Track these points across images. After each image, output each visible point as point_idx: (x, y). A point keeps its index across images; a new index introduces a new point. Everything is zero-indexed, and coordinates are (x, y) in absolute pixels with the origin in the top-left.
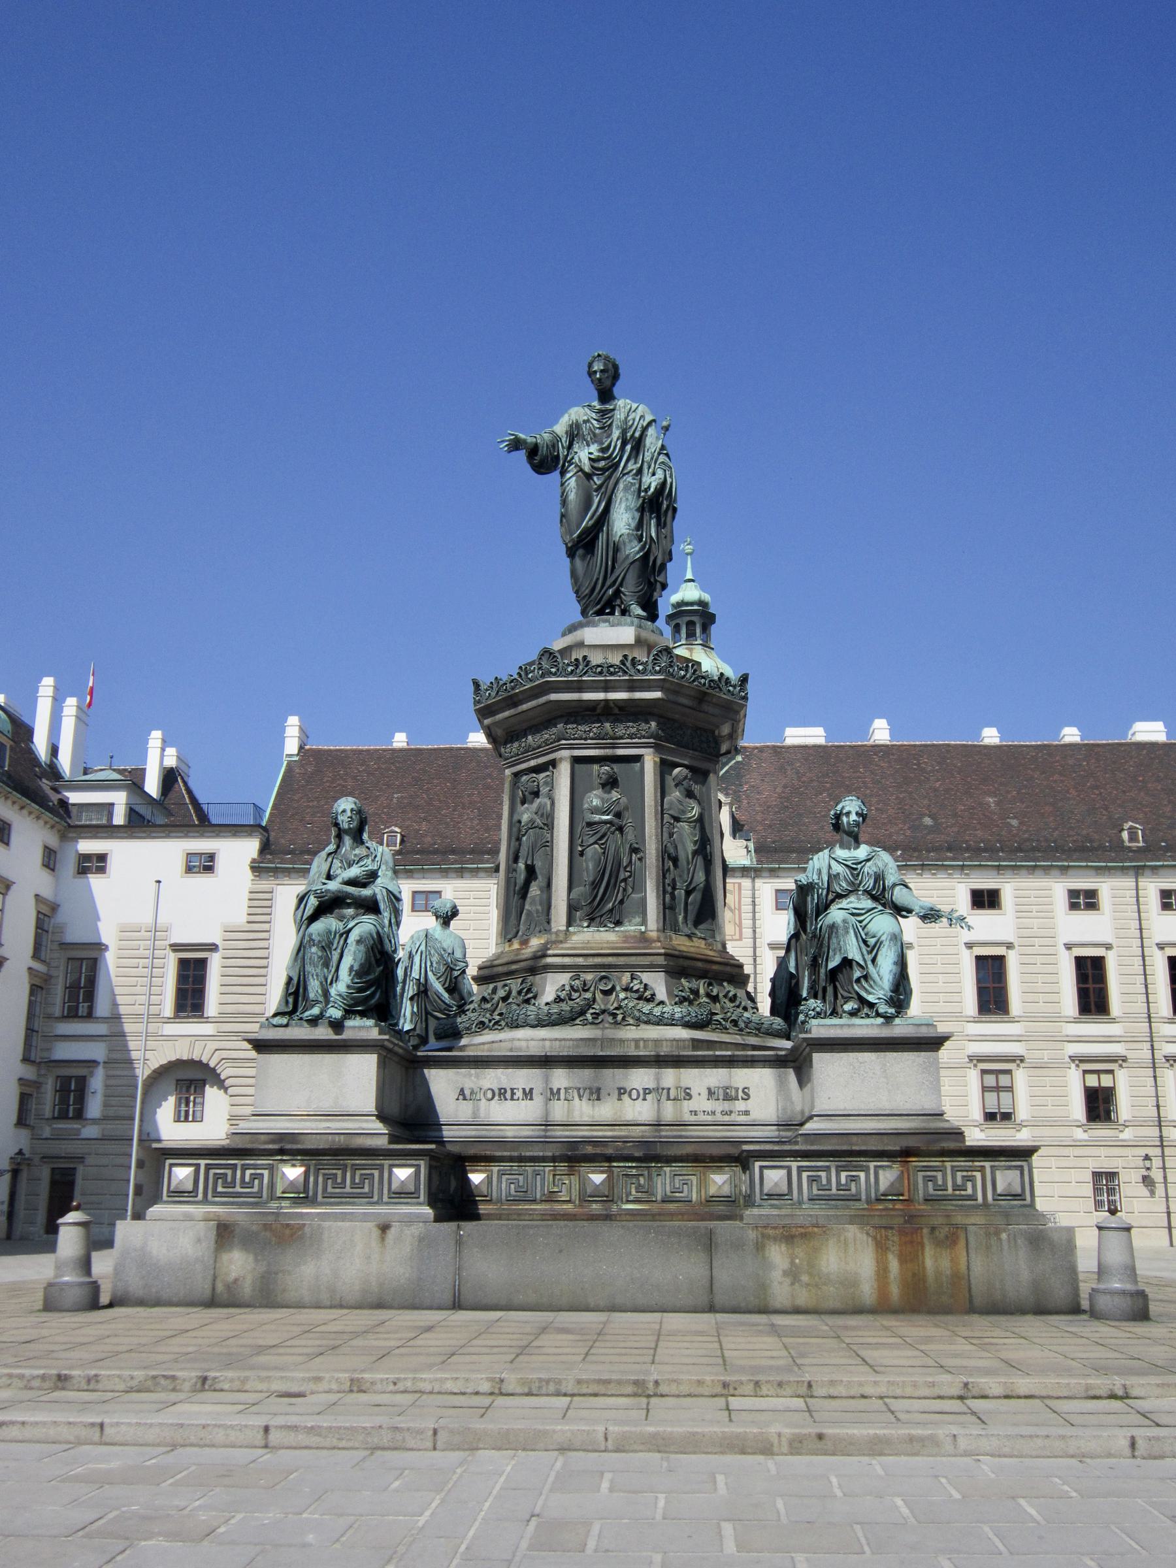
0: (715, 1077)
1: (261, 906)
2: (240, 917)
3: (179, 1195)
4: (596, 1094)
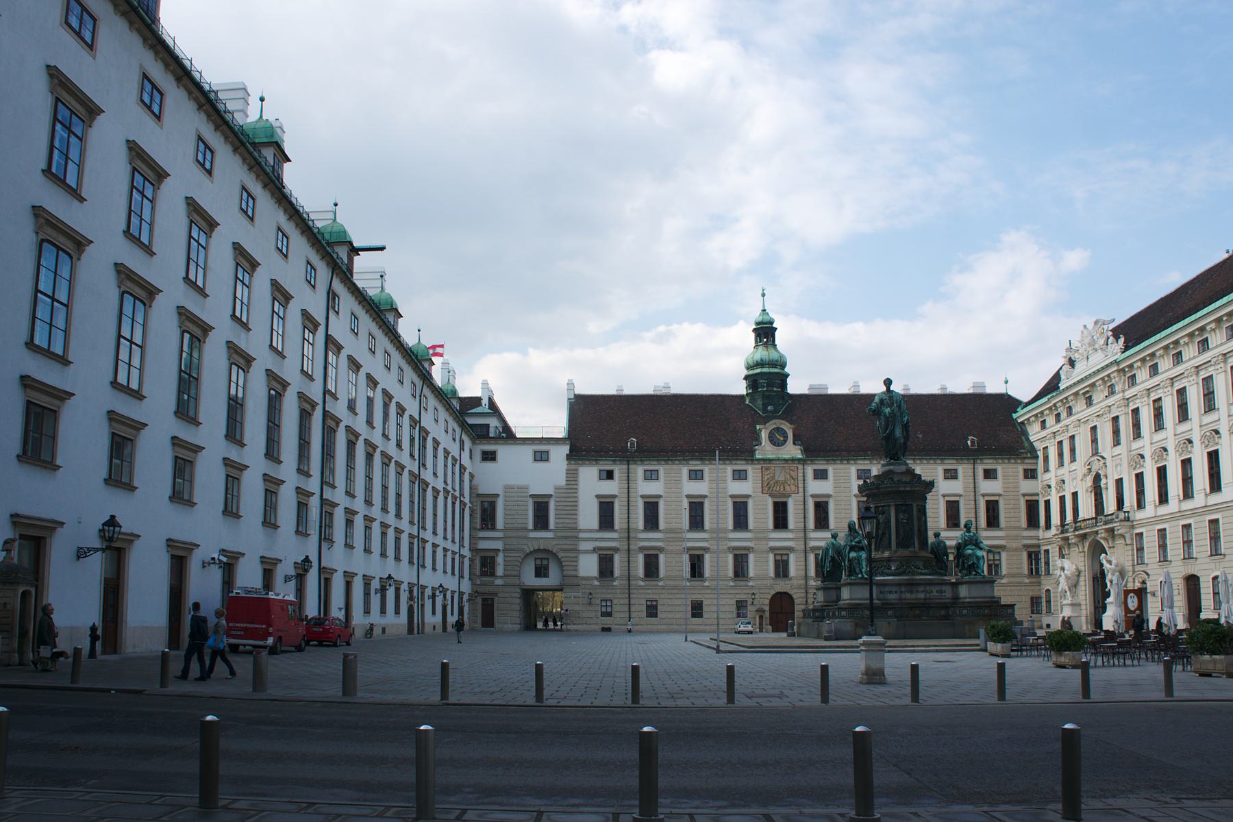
0: (938, 588)
1: (572, 477)
2: (562, 481)
3: (843, 617)
4: (911, 592)
